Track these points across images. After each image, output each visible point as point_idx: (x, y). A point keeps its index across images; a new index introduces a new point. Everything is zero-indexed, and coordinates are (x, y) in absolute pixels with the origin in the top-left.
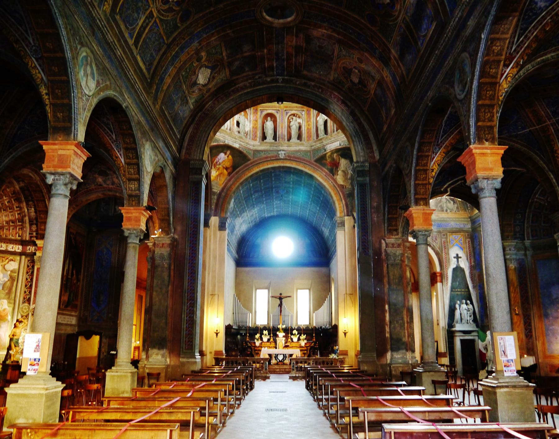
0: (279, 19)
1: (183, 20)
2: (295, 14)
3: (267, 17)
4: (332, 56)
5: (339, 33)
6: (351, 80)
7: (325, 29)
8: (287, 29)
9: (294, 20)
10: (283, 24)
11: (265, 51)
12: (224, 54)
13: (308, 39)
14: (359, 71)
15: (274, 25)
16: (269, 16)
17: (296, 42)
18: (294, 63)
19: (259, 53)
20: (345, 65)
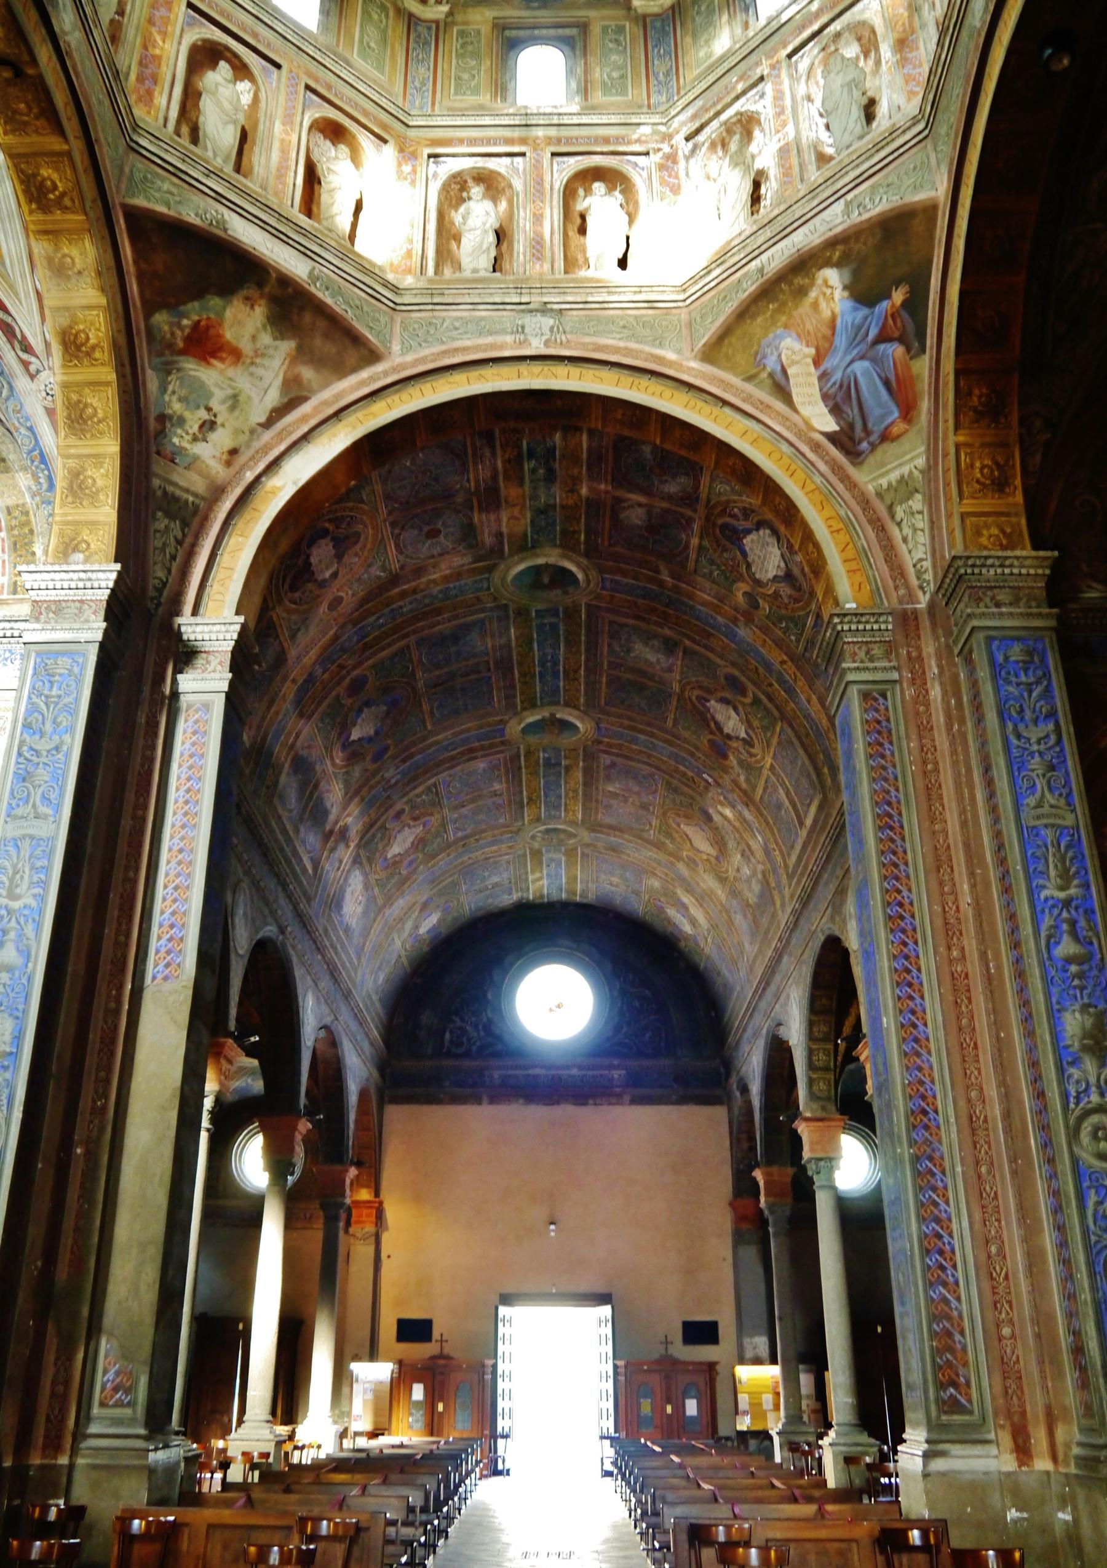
0: (547, 565)
1: (743, 692)
2: (509, 579)
3: (573, 568)
4: (397, 531)
5: (403, 595)
6: (324, 533)
7: (434, 581)
8: (524, 546)
9: (508, 569)
10: (537, 556)
11: (584, 491)
12: (695, 541)
13: (468, 535)
14: (323, 584)
15: (557, 551)
16: (570, 572)
17: (498, 520)
18: (499, 452)
19: (603, 487)
20: (357, 548)
